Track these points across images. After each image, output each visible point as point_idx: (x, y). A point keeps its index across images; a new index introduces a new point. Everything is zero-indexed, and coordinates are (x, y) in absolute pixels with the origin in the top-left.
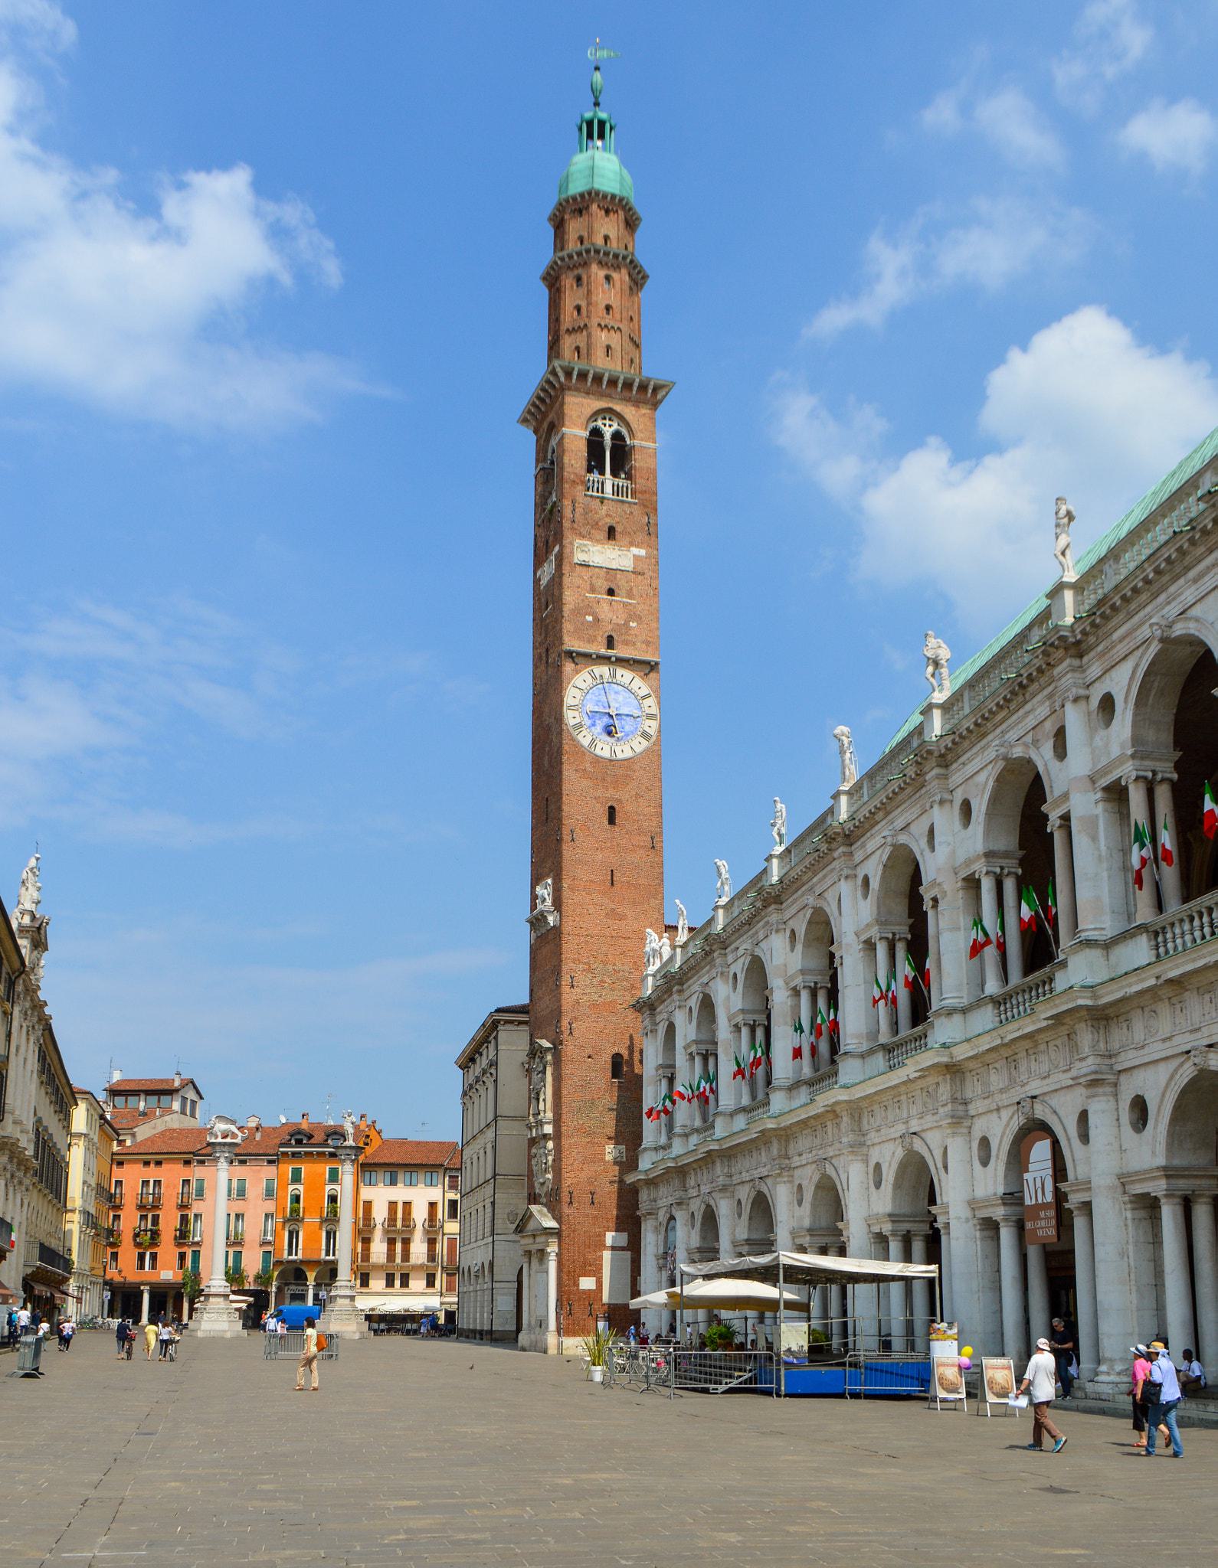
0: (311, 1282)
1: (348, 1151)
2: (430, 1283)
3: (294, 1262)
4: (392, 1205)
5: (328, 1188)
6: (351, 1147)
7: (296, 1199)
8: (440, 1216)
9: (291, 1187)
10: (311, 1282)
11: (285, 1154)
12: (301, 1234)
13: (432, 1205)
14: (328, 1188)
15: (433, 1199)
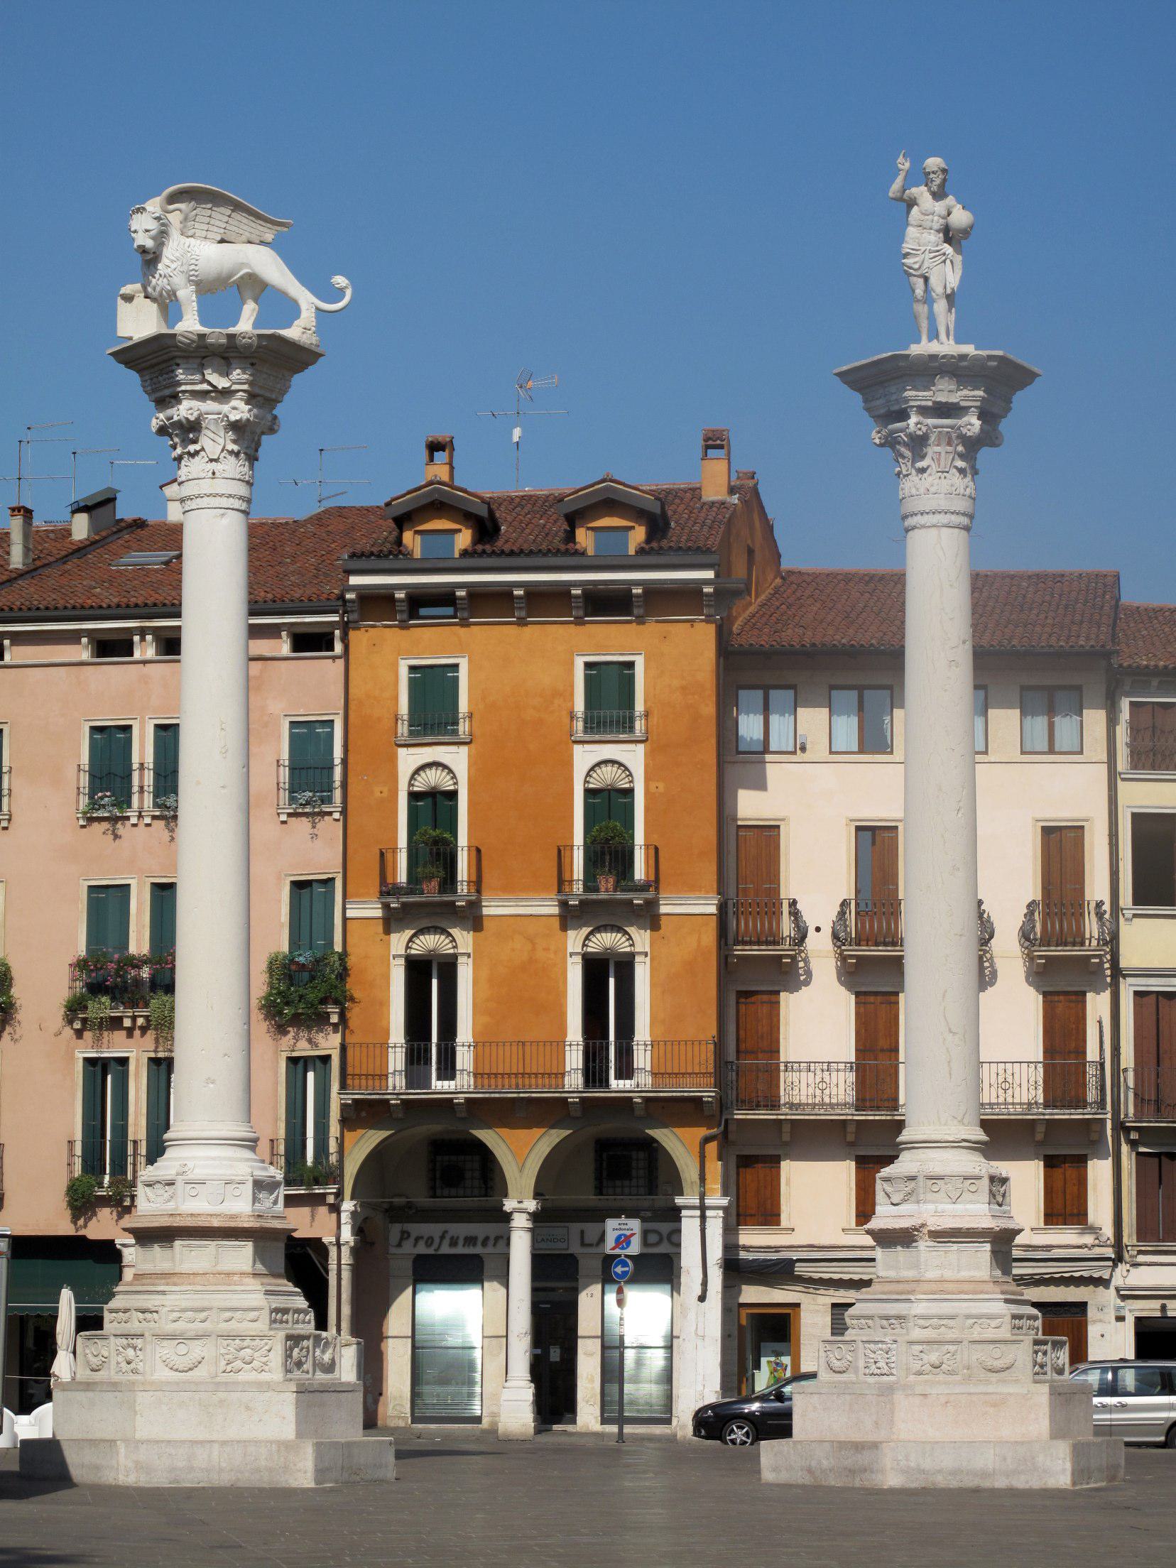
0: (520, 1204)
1: (945, 391)
2: (1064, 1206)
3: (444, 1105)
4: (876, 847)
5: (584, 757)
6: (957, 369)
7: (434, 807)
8: (1097, 888)
9: (408, 759)
10: (520, 1204)
11: (376, 605)
12: (465, 975)
13: (1060, 845)
14: (584, 757)
15: (1062, 814)
